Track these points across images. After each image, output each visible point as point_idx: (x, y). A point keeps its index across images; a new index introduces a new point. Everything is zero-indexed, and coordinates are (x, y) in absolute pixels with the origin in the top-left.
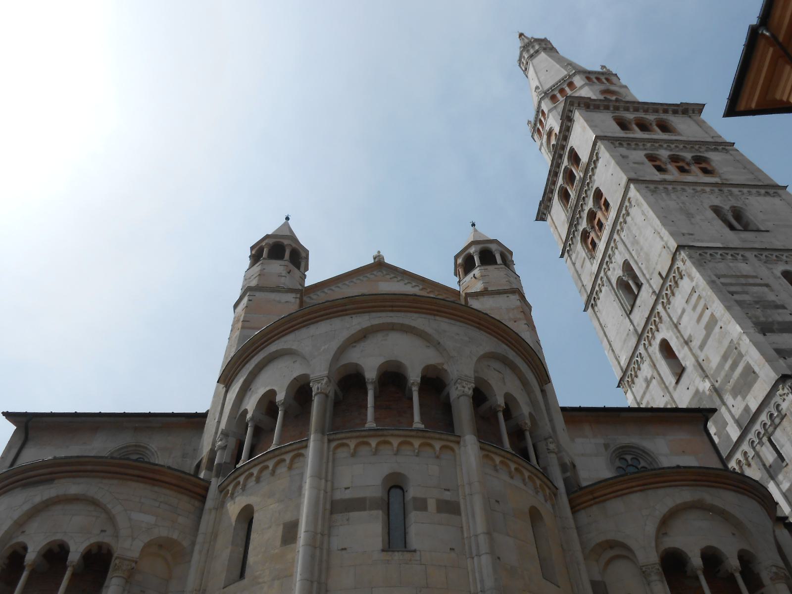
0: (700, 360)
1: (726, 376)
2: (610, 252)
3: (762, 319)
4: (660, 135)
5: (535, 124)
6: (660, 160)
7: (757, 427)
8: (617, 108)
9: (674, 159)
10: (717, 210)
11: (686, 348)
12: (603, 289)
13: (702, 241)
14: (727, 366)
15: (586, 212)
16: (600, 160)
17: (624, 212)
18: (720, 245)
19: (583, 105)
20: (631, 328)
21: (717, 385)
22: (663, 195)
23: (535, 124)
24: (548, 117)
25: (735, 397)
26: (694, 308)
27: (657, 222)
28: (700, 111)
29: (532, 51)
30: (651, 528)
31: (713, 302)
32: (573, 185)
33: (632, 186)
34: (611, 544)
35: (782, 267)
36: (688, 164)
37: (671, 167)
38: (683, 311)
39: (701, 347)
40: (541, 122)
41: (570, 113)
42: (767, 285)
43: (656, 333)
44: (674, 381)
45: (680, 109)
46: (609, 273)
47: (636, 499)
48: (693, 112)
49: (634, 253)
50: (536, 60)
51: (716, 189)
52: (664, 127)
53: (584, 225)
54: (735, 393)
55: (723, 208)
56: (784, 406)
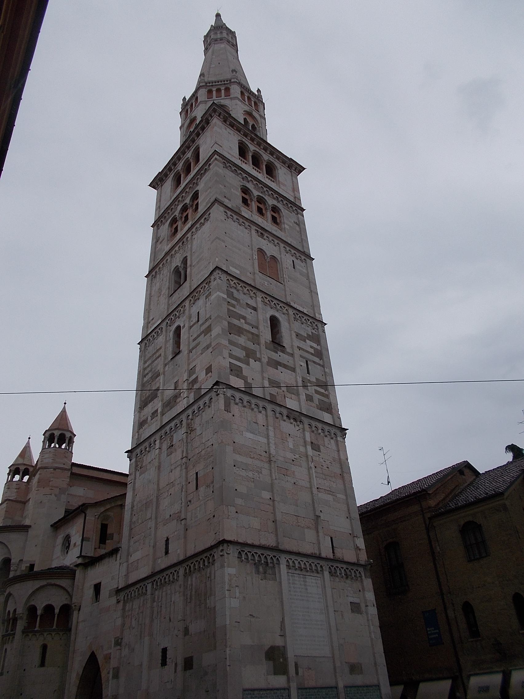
4: (262, 176)
5: (187, 104)
8: (246, 135)
9: (260, 200)
23: (187, 104)
24: (197, 107)
28: (300, 172)
29: (219, 36)
36: (266, 209)
37: (254, 205)
40: (192, 104)
41: (210, 118)
48: (295, 170)
50: (217, 47)
52: (270, 171)
55: (266, 254)
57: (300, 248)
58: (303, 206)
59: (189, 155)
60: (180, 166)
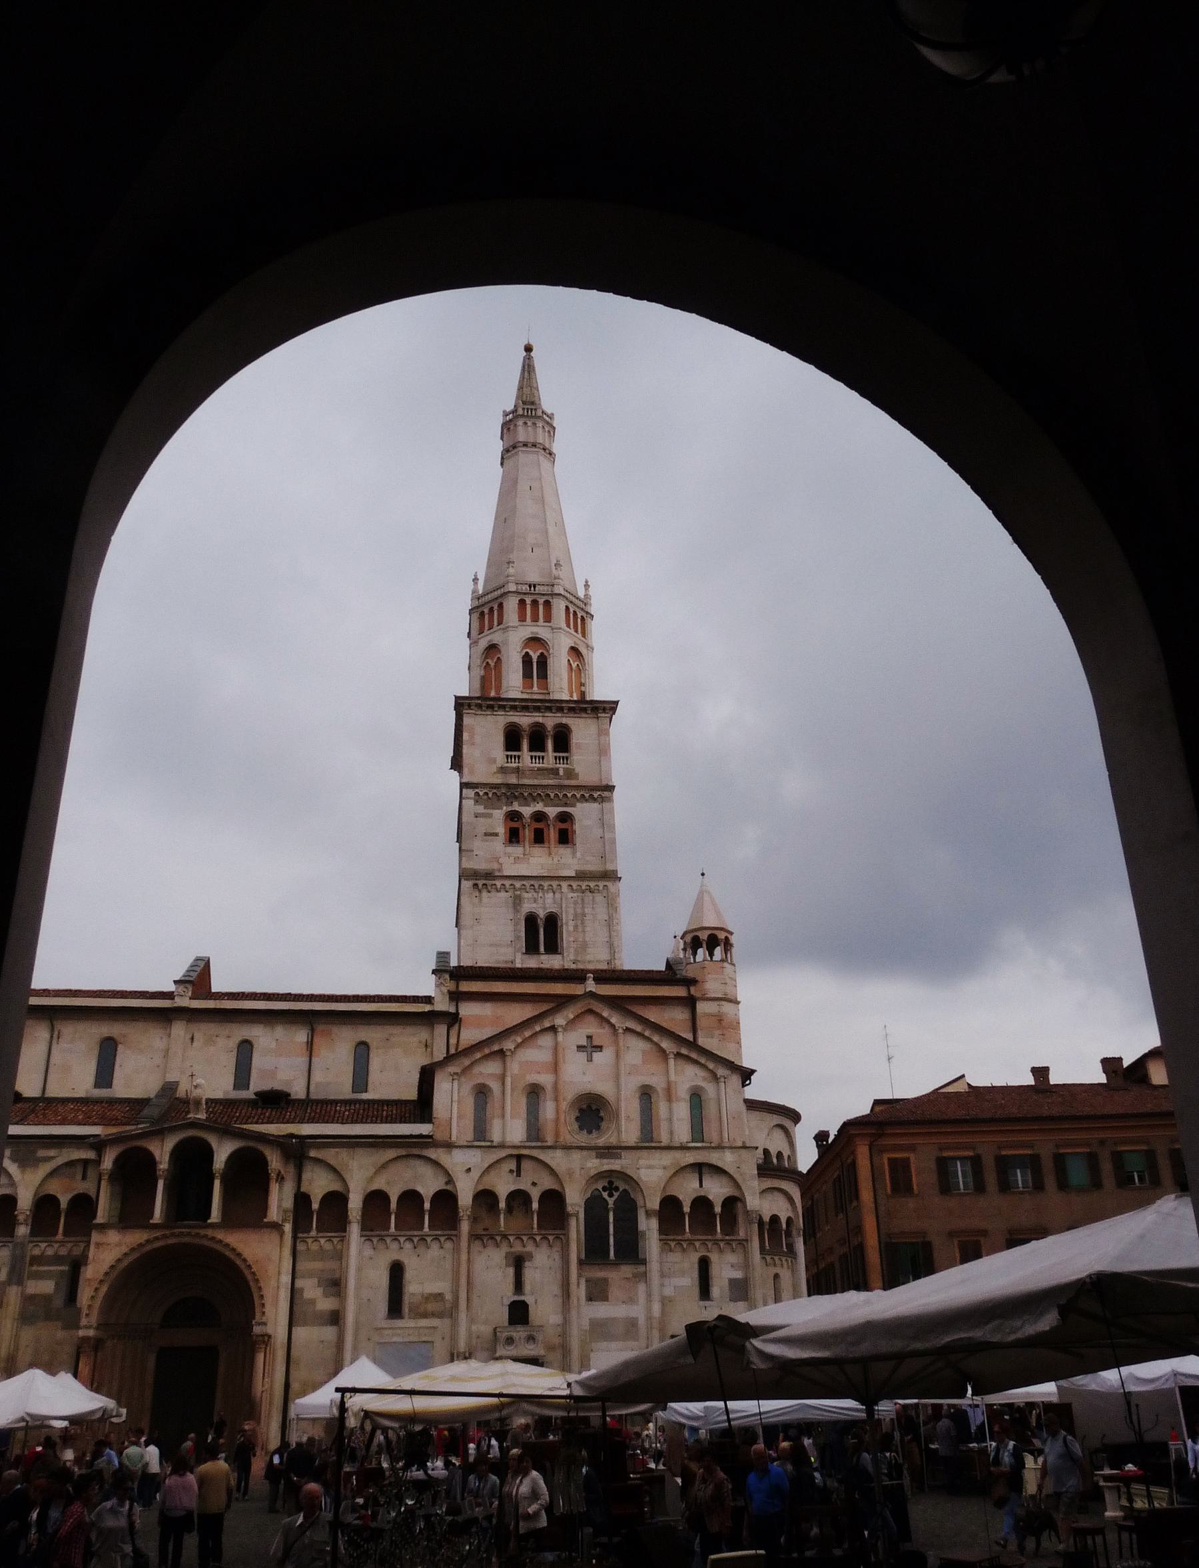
2: (546, 884)
12: (503, 894)
15: (539, 807)
16: (596, 805)
17: (592, 884)
49: (571, 923)
53: (527, 811)
60: (525, 720)
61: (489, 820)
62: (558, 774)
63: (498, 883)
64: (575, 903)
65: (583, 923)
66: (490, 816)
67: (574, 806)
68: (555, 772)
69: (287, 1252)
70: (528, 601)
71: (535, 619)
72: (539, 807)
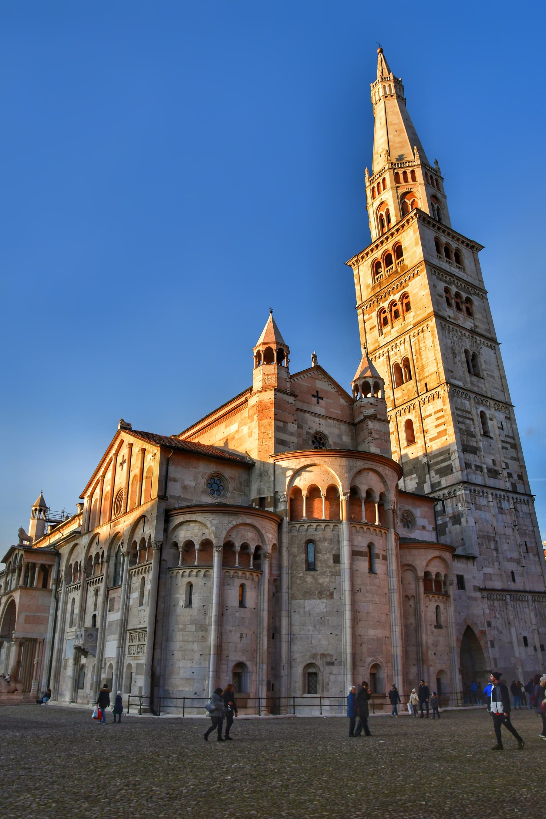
0: (427, 446)
1: (437, 462)
2: (398, 342)
3: (465, 443)
6: (450, 294)
7: (441, 493)
8: (439, 228)
9: (457, 295)
10: (466, 352)
11: (422, 434)
12: (382, 358)
13: (455, 379)
14: (440, 458)
15: (392, 298)
16: (418, 277)
18: (460, 384)
19: (422, 219)
20: (392, 397)
21: (430, 463)
22: (447, 331)
25: (437, 473)
26: (437, 419)
27: (439, 356)
30: (424, 563)
31: (450, 425)
32: (387, 267)
33: (434, 319)
34: (409, 565)
35: (481, 408)
38: (430, 415)
39: (431, 440)
40: (379, 183)
42: (473, 420)
43: (407, 412)
44: (405, 444)
45: (471, 244)
46: (391, 353)
47: (422, 551)
49: (415, 358)
51: (470, 335)
53: (385, 305)
54: (438, 472)
56: (458, 493)
57: (489, 335)
58: (487, 288)
59: (389, 246)
60: (378, 254)
61: (371, 320)
62: (397, 272)
63: (377, 354)
64: (416, 343)
65: (420, 355)
66: (371, 318)
67: (408, 285)
68: (396, 272)
69: (53, 599)
70: (375, 185)
71: (379, 193)
72: (392, 298)
